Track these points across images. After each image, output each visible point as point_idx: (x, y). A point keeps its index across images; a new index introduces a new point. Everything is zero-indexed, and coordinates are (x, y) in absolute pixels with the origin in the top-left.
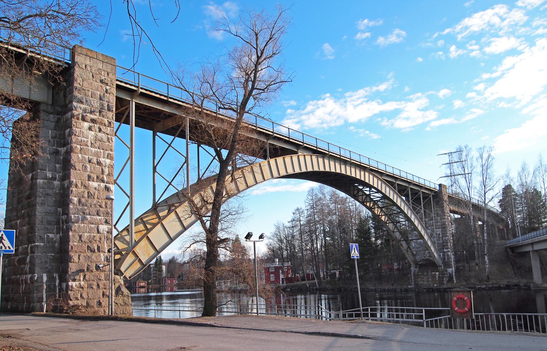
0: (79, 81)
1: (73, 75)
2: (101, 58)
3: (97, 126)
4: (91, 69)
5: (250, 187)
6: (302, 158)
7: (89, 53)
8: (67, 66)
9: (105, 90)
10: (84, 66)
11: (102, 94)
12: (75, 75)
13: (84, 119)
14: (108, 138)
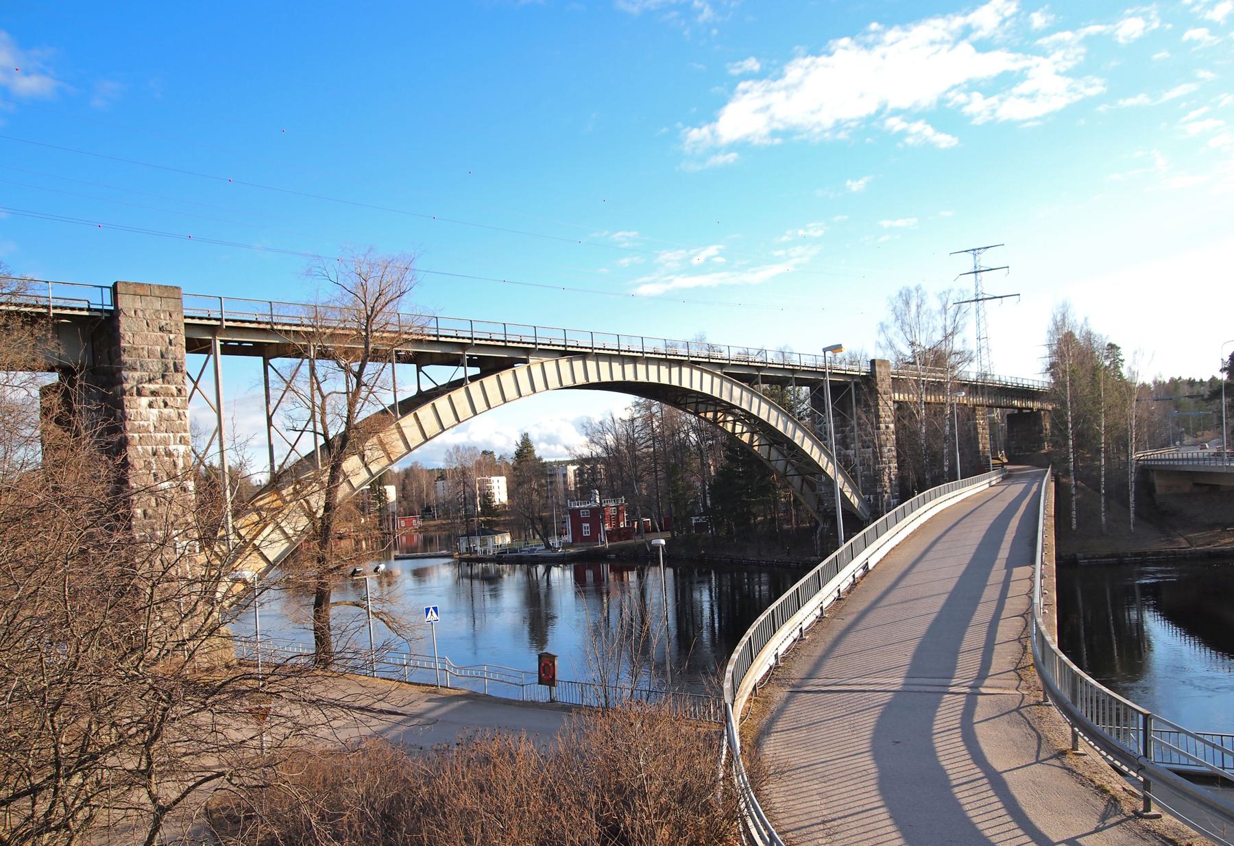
0: (127, 338)
1: (118, 330)
2: (157, 293)
3: (160, 399)
4: (144, 315)
5: (431, 438)
6: (536, 370)
7: (139, 291)
8: (107, 315)
9: (168, 341)
10: (133, 313)
11: (164, 349)
12: (121, 330)
13: (139, 394)
14: (179, 414)
